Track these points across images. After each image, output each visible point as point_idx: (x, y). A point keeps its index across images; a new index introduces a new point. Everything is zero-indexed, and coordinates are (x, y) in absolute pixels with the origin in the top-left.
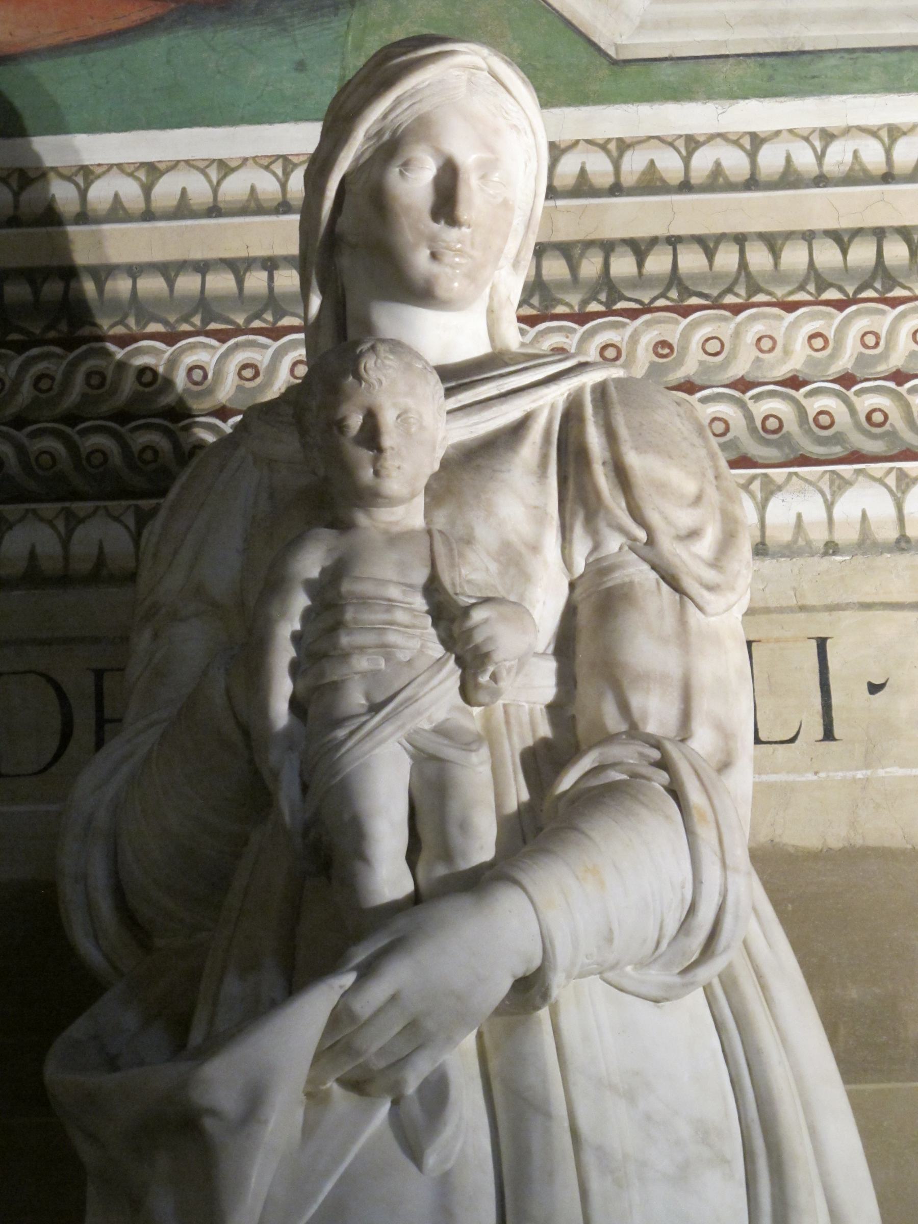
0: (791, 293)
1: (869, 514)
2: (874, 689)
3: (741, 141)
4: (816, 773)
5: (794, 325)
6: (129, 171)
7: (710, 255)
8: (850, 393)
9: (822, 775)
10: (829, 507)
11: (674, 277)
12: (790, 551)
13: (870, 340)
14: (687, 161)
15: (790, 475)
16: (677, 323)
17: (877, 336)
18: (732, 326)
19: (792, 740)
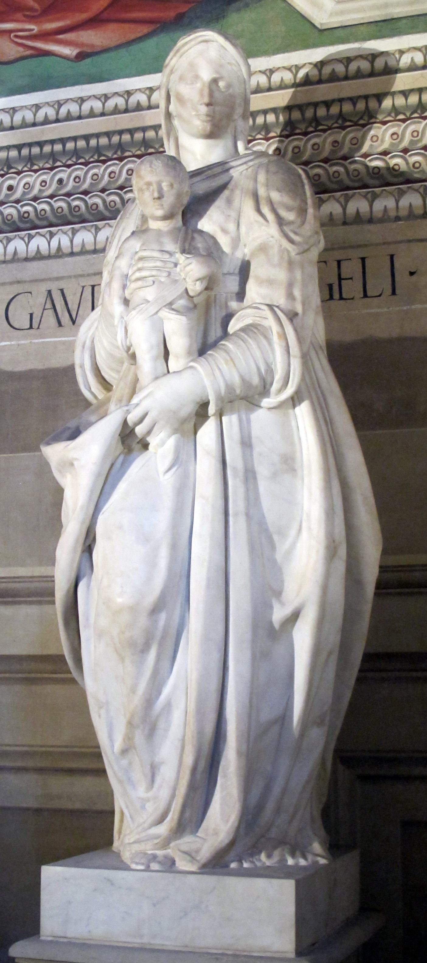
0: (385, 117)
1: (412, 204)
2: (412, 274)
3: (368, 58)
4: (388, 308)
5: (386, 130)
6: (143, 91)
7: (354, 104)
8: (407, 156)
9: (391, 309)
10: (397, 202)
11: (341, 115)
12: (381, 221)
13: (415, 134)
14: (347, 67)
15: (330, 197)
16: (341, 133)
17: (418, 132)
18: (362, 133)
19: (380, 296)
